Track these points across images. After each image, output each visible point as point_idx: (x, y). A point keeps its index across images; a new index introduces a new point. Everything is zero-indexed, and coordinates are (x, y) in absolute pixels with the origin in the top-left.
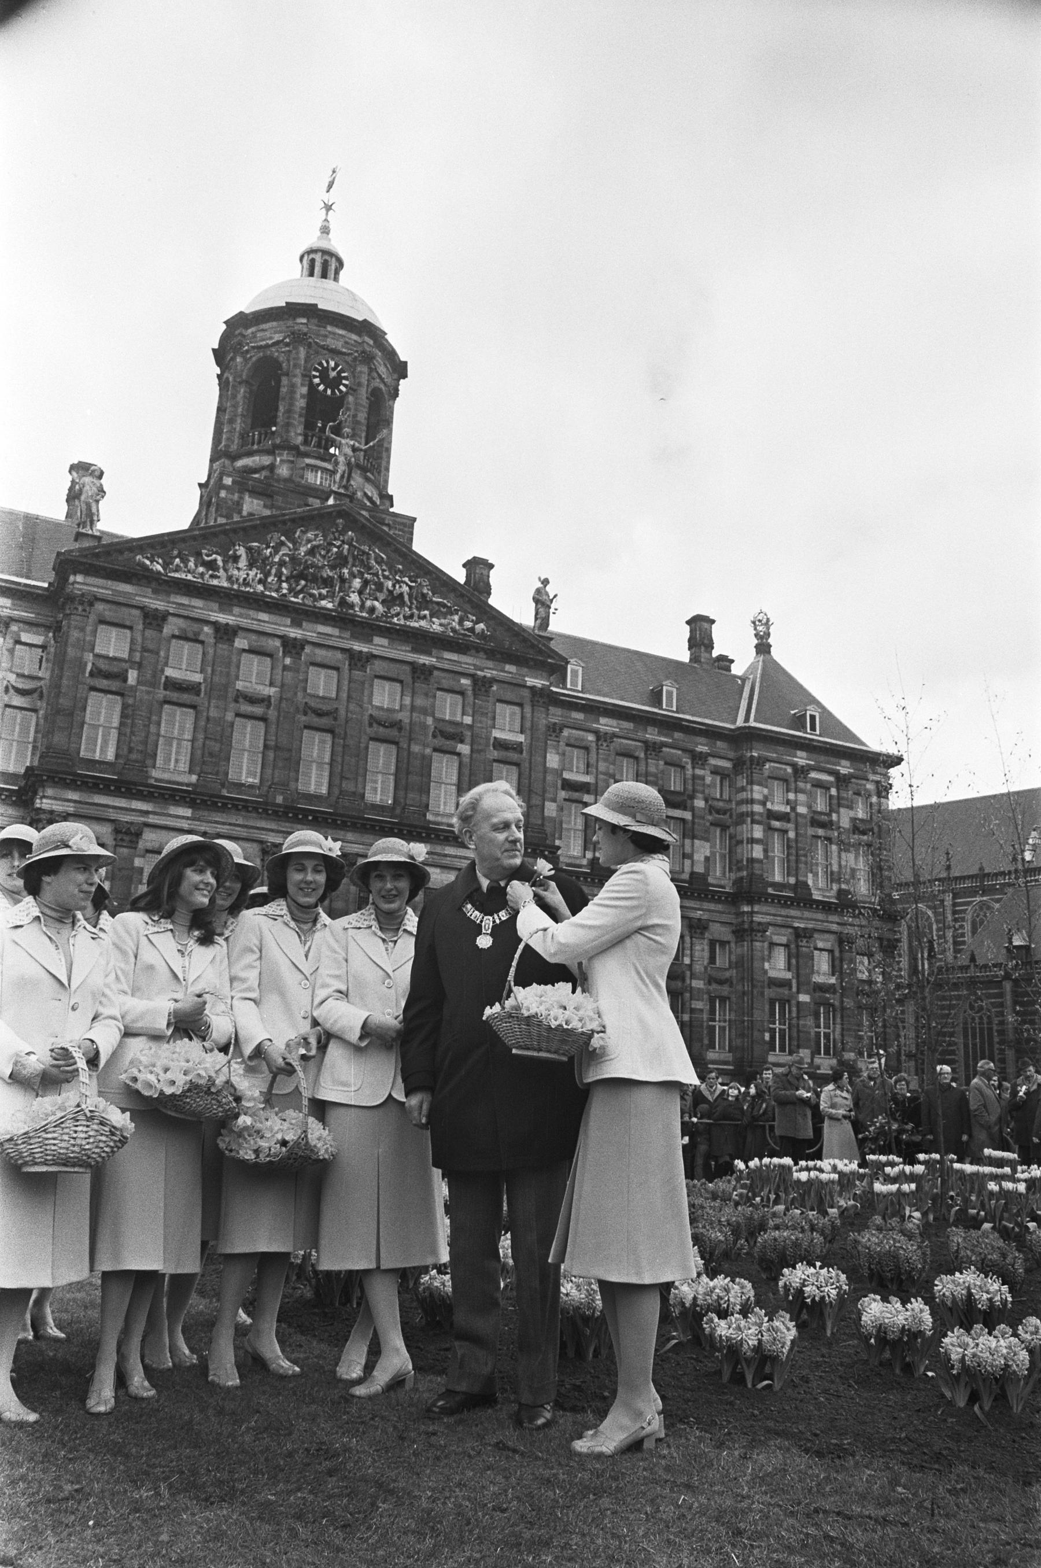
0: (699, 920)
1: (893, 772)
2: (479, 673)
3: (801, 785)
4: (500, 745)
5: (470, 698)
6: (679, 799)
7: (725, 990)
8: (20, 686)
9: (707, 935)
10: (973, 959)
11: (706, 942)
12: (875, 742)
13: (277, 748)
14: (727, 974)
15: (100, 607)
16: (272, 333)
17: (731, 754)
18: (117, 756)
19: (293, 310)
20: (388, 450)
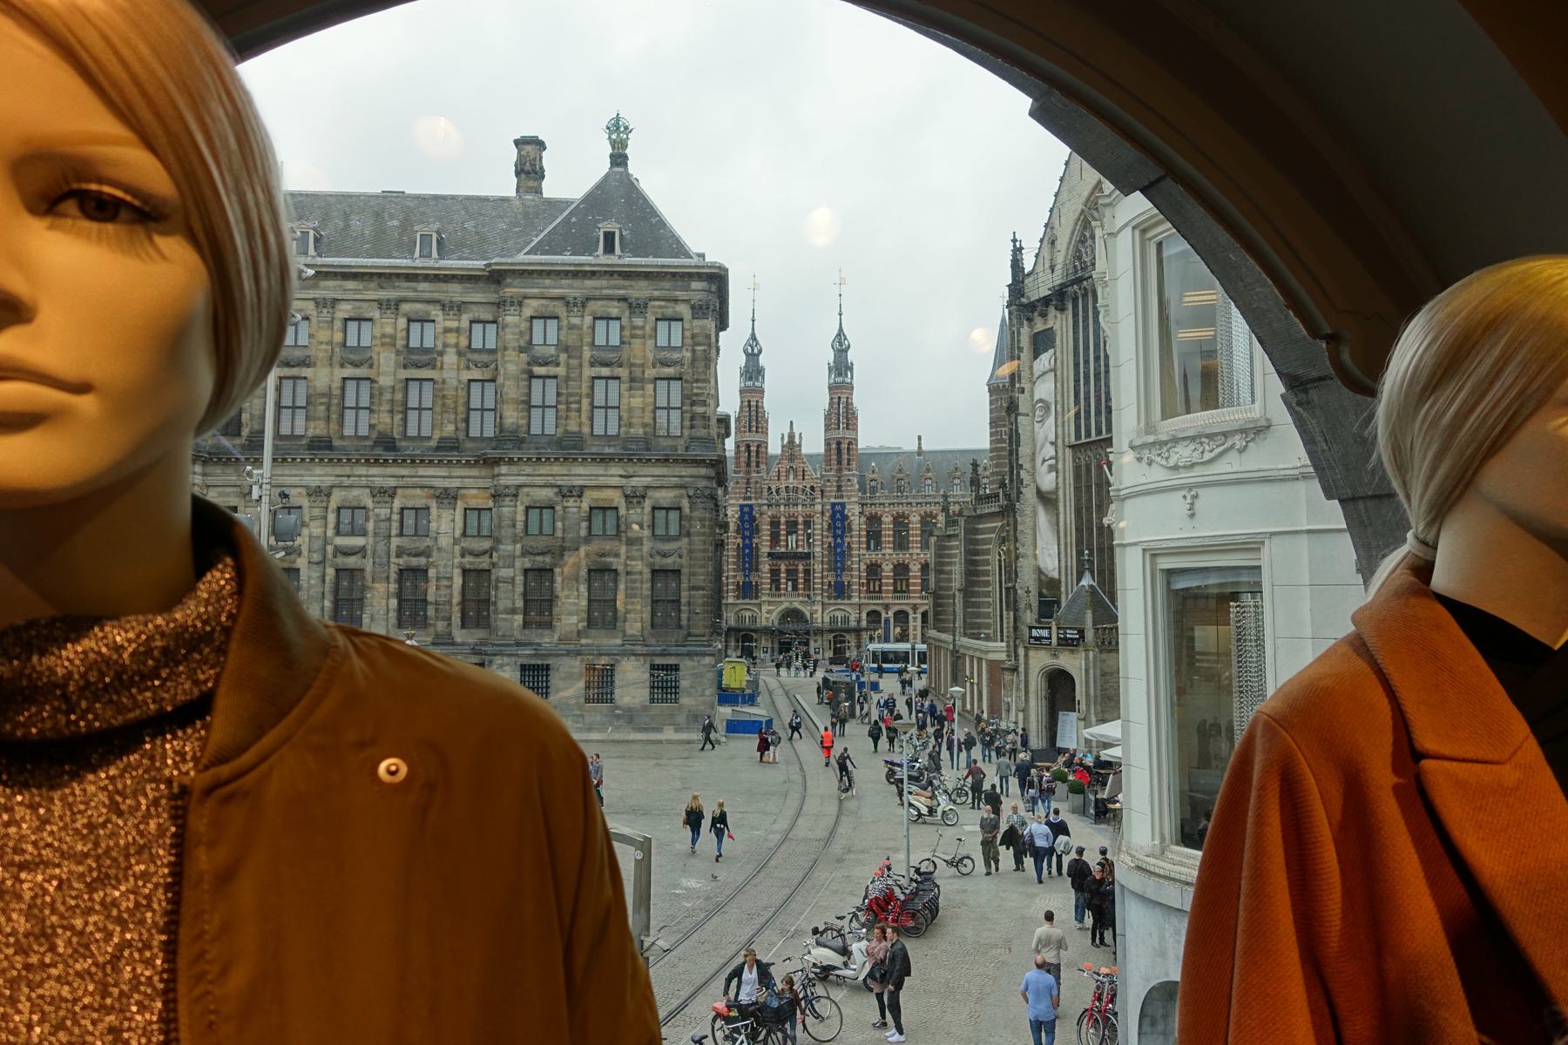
0: (446, 489)
3: (576, 321)
6: (424, 358)
9: (459, 503)
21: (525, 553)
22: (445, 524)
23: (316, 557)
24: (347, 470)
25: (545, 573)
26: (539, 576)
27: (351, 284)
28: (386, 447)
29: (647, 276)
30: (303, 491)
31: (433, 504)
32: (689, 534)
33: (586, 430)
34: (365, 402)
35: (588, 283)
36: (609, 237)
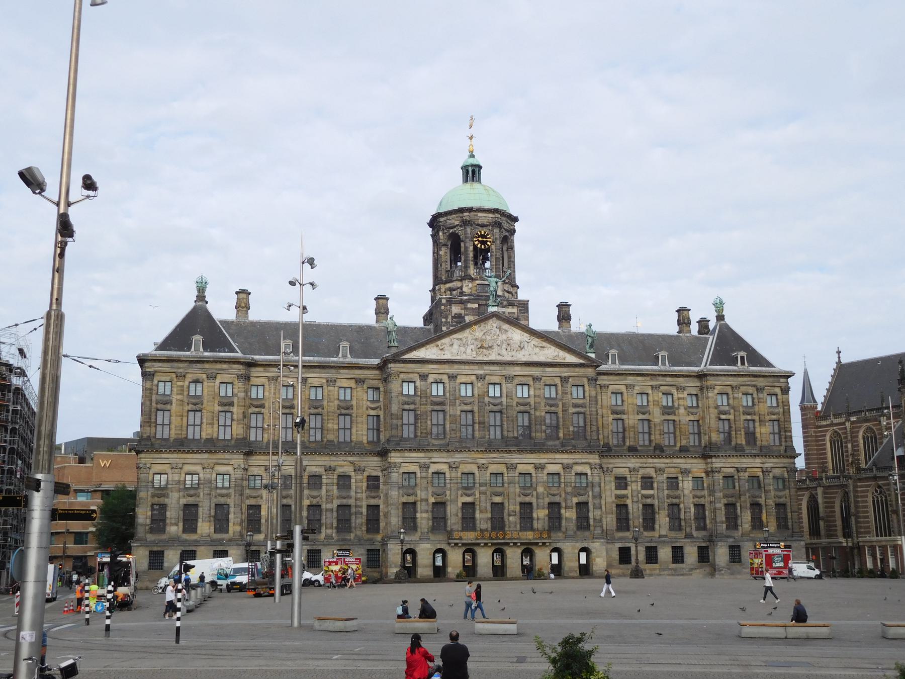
1: (790, 380)
2: (563, 375)
3: (736, 395)
4: (575, 406)
5: (560, 387)
7: (702, 501)
8: (373, 406)
10: (874, 464)
11: (690, 478)
12: (780, 364)
13: (479, 423)
14: (703, 493)
15: (402, 376)
16: (455, 221)
17: (698, 384)
18: (416, 436)
19: (461, 211)
20: (514, 262)
21: (725, 496)
22: (687, 485)
23: (635, 499)
24: (644, 460)
25: (734, 505)
26: (730, 506)
27: (640, 378)
28: (659, 451)
29: (764, 376)
30: (627, 470)
31: (680, 475)
32: (789, 489)
33: (744, 443)
34: (646, 430)
35: (740, 379)
36: (742, 358)
